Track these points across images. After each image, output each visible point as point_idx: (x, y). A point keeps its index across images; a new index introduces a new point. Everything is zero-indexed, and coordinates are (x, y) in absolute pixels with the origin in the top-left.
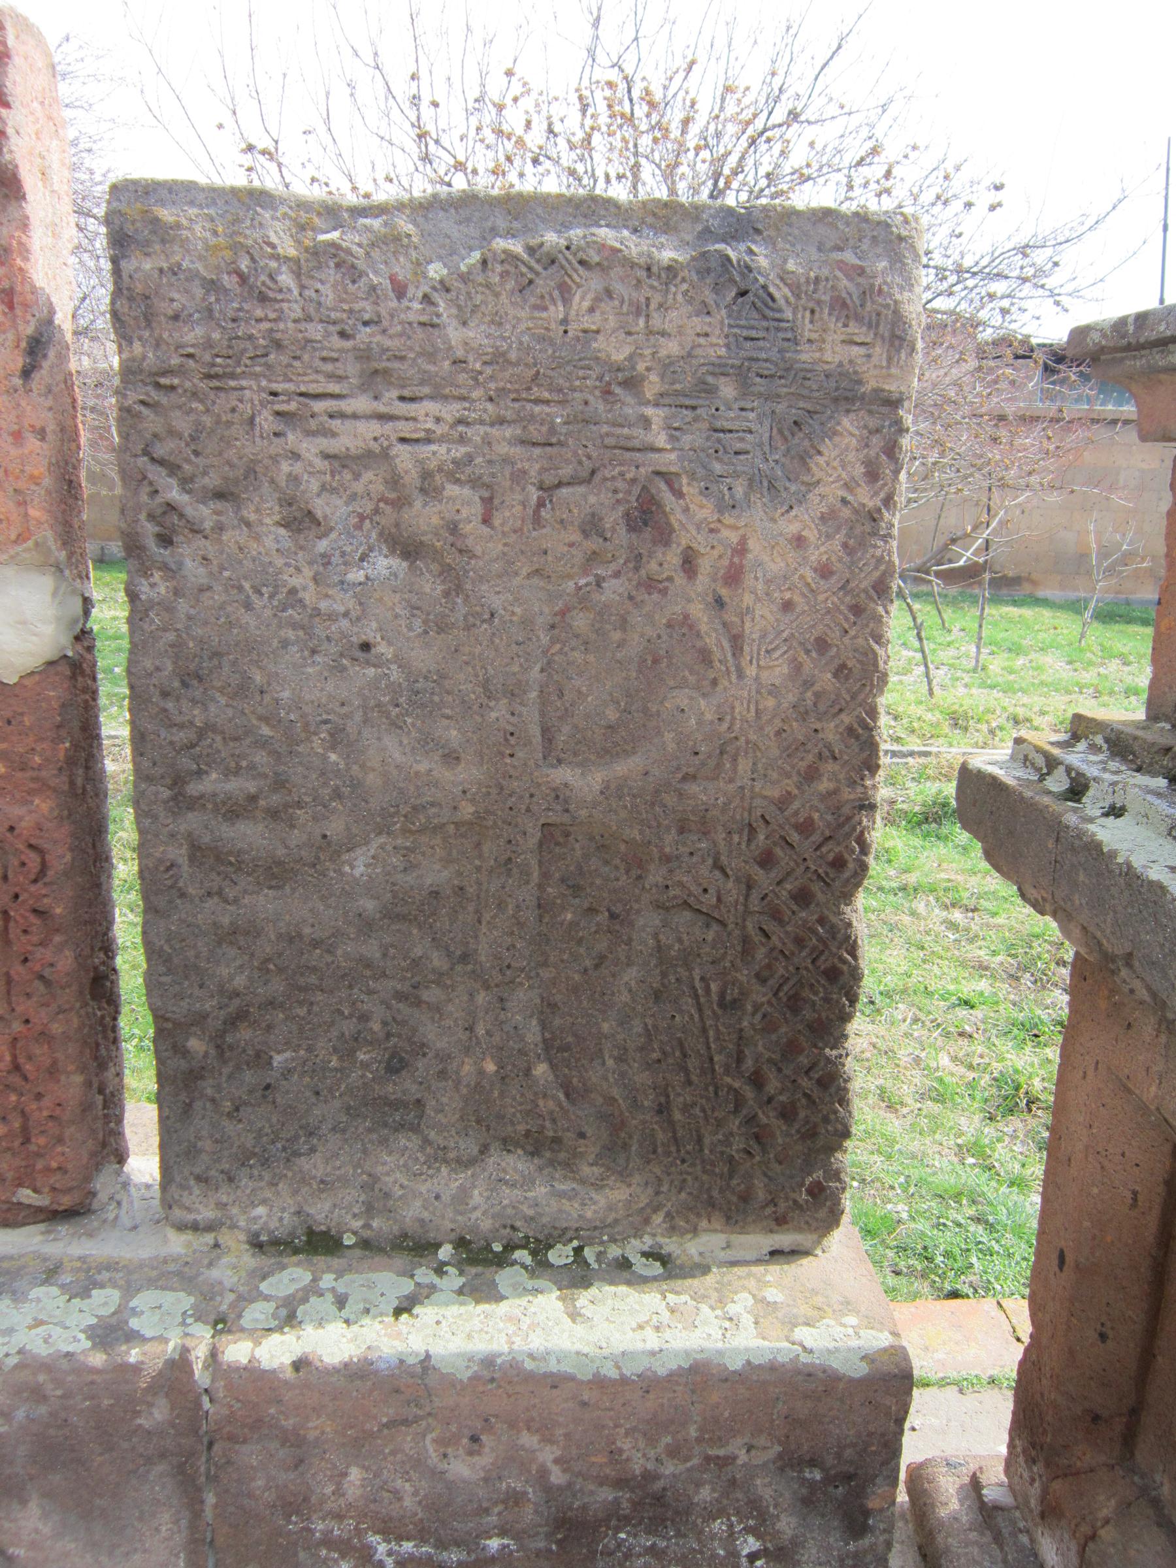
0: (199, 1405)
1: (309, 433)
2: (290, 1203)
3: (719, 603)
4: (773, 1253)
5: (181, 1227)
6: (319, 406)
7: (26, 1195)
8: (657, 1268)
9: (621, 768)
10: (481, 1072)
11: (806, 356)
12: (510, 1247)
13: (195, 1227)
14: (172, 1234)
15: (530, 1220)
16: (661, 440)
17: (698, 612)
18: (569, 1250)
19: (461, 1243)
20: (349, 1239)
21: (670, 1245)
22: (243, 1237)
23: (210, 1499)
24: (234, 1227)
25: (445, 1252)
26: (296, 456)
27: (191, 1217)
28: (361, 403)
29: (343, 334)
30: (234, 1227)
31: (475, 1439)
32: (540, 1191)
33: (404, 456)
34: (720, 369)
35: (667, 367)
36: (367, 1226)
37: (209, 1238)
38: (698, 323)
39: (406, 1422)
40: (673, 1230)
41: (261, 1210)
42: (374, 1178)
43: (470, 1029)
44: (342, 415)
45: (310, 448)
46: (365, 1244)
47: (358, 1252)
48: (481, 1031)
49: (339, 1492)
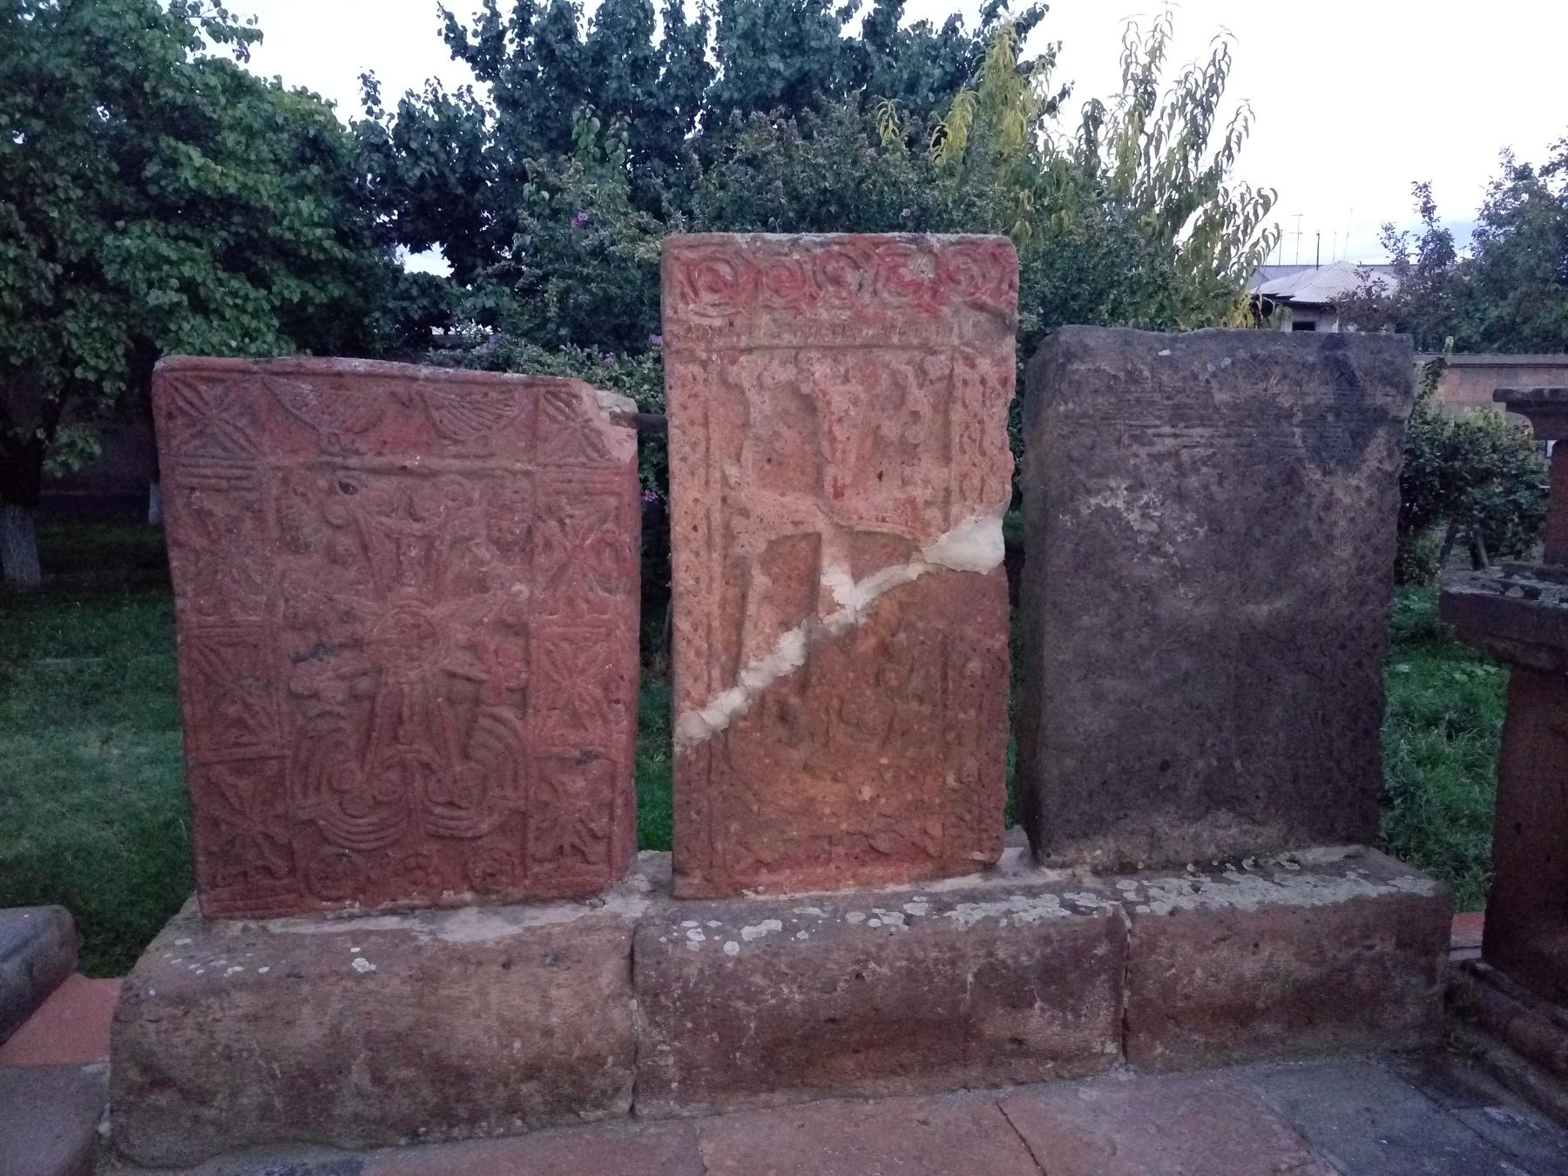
0: (1125, 939)
1: (1143, 445)
2: (1112, 844)
3: (1320, 520)
4: (1348, 857)
5: (1052, 867)
6: (1150, 431)
7: (978, 856)
8: (1296, 867)
9: (1278, 604)
10: (1210, 766)
11: (1368, 401)
12: (1222, 863)
13: (1063, 866)
14: (1047, 871)
15: (1231, 846)
16: (1299, 443)
17: (1311, 524)
18: (1250, 862)
19: (1196, 863)
20: (1140, 866)
21: (1298, 854)
22: (1087, 868)
23: (1127, 993)
24: (1085, 862)
25: (1190, 868)
26: (1136, 455)
27: (1060, 859)
28: (1167, 430)
29: (1168, 398)
30: (1085, 862)
31: (1256, 945)
32: (1234, 831)
33: (1185, 454)
34: (1330, 409)
35: (1305, 409)
36: (1150, 858)
37: (1069, 871)
38: (1323, 389)
39: (1224, 939)
40: (1298, 848)
41: (1099, 852)
42: (1154, 830)
43: (1203, 745)
44: (1159, 435)
45: (1143, 452)
46: (1148, 867)
47: (1147, 872)
48: (1208, 744)
49: (1191, 982)
